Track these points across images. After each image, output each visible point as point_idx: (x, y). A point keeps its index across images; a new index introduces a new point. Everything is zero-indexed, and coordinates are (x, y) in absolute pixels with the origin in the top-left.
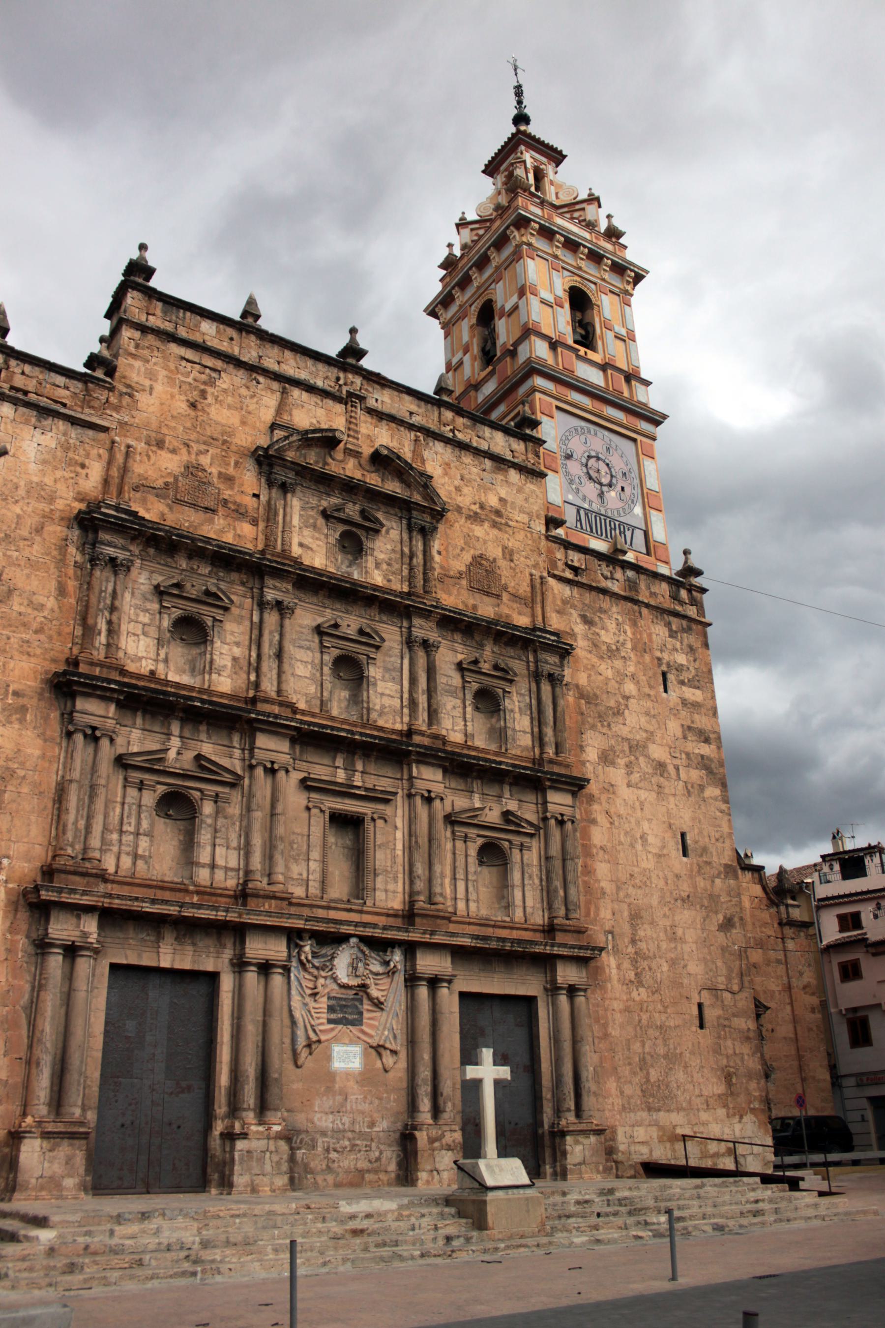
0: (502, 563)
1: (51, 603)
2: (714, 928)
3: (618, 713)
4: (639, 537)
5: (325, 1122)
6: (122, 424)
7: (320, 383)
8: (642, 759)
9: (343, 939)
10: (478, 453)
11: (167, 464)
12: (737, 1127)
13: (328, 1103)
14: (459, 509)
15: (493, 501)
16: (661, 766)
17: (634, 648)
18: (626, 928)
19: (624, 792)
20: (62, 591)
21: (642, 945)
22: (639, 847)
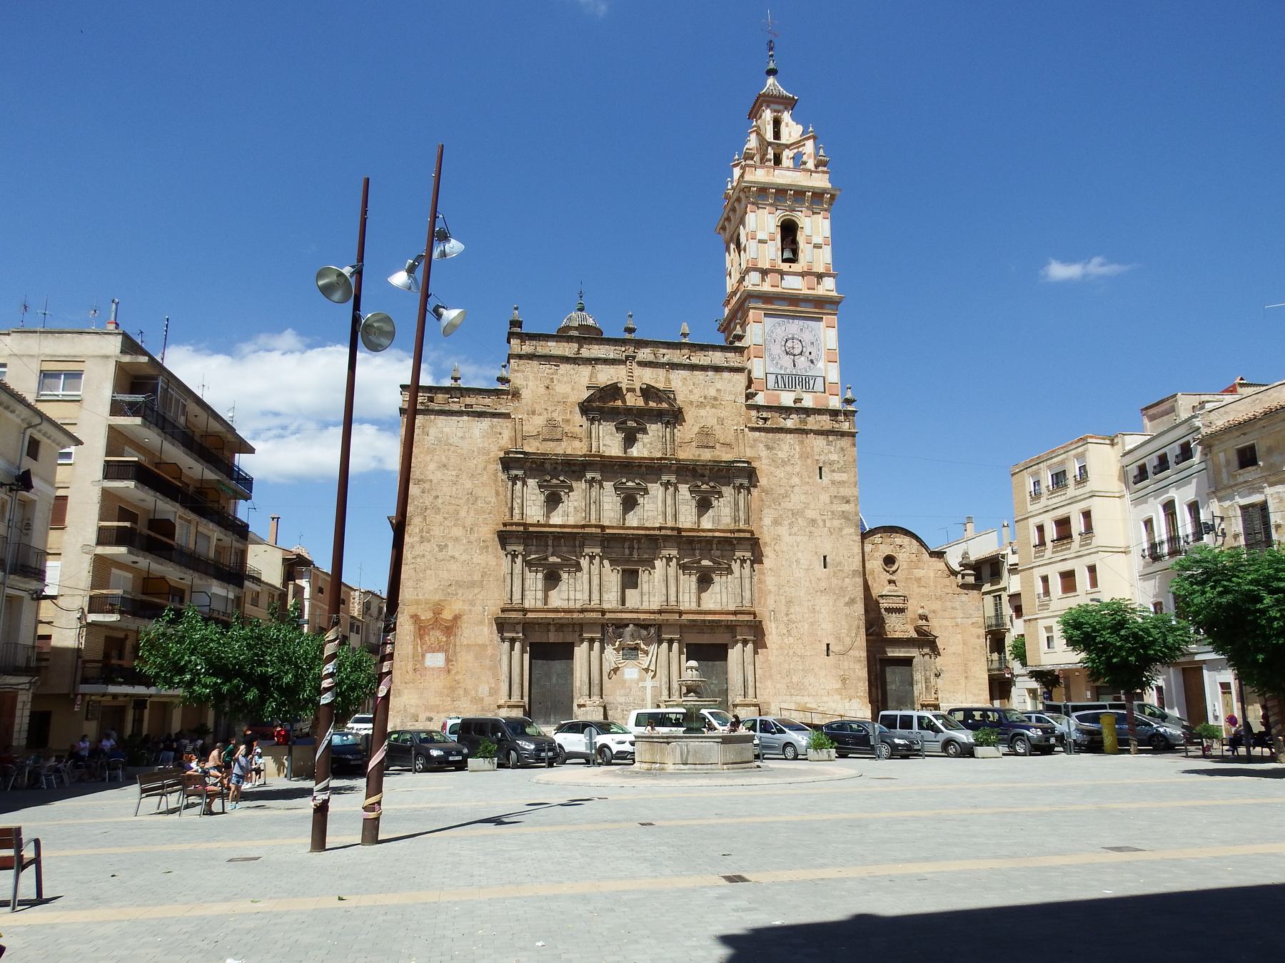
0: (717, 427)
1: (494, 500)
2: (841, 605)
3: (786, 496)
4: (819, 381)
5: (622, 700)
6: (516, 408)
7: (611, 356)
8: (800, 520)
9: (627, 625)
10: (704, 368)
11: (538, 422)
12: (847, 705)
13: (622, 692)
14: (691, 403)
15: (712, 392)
16: (813, 521)
17: (801, 457)
18: (784, 609)
19: (787, 539)
20: (497, 494)
21: (793, 617)
22: (794, 566)
